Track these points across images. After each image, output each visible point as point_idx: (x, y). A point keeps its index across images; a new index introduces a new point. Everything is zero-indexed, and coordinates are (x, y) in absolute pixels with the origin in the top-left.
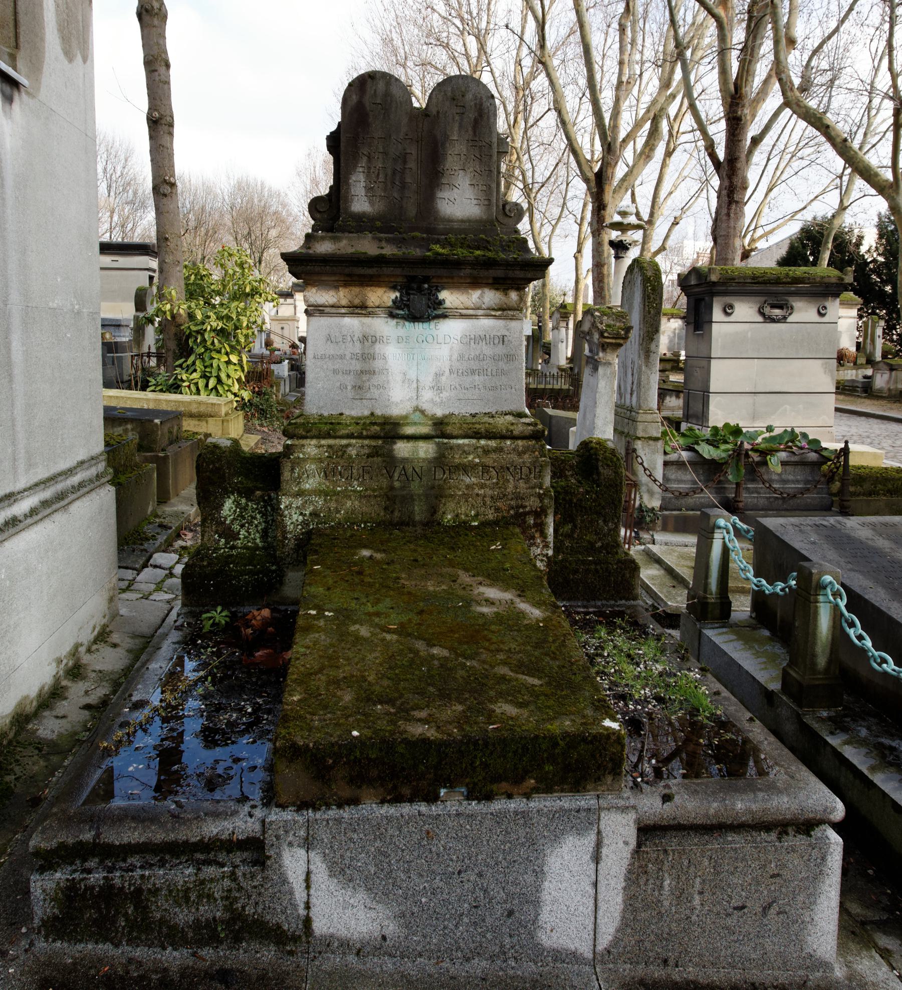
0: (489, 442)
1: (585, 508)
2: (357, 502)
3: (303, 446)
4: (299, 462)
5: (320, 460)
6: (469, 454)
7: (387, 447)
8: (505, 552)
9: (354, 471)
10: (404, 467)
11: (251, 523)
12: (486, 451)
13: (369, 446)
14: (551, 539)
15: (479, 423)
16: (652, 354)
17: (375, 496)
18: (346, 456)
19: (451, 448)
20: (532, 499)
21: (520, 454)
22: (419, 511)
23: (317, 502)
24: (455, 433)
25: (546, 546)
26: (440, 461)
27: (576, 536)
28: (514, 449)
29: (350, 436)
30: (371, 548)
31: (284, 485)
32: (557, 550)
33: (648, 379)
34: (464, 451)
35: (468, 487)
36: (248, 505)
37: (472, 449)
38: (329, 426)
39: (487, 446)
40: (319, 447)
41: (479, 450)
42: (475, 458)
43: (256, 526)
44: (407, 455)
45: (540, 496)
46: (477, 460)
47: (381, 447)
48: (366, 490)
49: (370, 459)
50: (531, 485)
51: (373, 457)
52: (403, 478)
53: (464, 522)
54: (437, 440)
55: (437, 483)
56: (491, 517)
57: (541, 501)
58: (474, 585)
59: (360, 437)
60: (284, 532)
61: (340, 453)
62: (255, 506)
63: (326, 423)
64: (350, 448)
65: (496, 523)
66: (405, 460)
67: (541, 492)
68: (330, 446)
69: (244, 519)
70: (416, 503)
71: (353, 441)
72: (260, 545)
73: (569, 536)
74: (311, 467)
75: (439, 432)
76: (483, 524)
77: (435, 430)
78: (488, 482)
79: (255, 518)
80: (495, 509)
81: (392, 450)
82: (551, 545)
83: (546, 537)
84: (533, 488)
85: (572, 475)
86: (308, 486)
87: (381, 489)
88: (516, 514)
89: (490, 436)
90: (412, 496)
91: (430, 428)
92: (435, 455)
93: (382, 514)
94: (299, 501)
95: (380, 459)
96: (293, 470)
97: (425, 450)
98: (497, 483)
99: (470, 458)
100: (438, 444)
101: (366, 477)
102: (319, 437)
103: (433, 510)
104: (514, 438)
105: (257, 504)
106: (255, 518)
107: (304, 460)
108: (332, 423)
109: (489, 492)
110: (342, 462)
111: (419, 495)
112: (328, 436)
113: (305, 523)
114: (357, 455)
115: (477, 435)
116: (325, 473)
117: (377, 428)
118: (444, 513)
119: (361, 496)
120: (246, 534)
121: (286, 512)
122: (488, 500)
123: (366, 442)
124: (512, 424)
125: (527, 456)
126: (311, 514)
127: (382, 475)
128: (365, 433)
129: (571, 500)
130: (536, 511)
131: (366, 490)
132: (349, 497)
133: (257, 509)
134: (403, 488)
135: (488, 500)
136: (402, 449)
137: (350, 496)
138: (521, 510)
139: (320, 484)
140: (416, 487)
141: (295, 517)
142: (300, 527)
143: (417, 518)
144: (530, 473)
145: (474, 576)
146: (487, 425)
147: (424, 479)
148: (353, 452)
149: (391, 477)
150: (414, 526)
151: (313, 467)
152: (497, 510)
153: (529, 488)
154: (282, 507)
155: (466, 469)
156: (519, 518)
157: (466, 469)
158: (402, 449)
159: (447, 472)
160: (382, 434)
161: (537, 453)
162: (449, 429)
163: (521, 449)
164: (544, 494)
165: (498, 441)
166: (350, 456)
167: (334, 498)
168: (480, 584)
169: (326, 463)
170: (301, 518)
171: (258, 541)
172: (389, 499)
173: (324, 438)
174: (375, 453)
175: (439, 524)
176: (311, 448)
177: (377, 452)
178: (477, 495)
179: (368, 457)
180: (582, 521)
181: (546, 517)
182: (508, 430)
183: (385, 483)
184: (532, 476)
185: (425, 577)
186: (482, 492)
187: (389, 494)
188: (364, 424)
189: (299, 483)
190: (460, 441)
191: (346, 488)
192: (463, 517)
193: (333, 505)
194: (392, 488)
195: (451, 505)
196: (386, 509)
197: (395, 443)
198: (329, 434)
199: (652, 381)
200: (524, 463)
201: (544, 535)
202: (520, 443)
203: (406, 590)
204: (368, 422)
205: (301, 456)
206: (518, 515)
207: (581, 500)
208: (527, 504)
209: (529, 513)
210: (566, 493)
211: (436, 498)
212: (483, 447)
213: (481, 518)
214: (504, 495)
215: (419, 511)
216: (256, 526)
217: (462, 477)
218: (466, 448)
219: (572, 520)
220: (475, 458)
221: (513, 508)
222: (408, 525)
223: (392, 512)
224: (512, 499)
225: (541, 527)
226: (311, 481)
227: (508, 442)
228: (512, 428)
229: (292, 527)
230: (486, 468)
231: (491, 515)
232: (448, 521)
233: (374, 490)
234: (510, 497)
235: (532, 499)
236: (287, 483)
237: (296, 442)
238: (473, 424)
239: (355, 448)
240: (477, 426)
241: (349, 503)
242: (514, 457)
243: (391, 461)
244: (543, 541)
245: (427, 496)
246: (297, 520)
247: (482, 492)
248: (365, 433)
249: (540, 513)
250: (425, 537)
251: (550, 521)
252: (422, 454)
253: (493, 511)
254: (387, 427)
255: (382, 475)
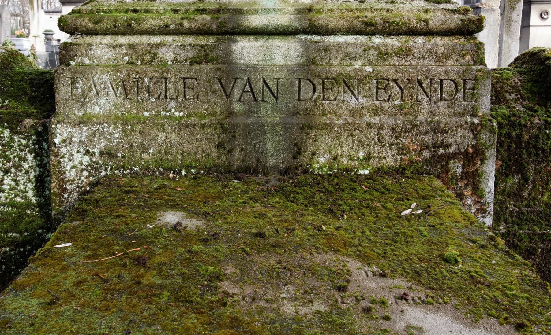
0: (389, 41)
1: (543, 151)
2: (174, 135)
3: (90, 45)
4: (82, 71)
5: (117, 68)
6: (355, 58)
7: (222, 46)
8: (432, 220)
9: (169, 86)
10: (248, 79)
11: (18, 167)
12: (383, 55)
13: (192, 46)
14: (490, 199)
15: (371, 10)
16: (513, 23)
17: (203, 126)
18: (156, 62)
19: (326, 49)
20: (460, 132)
21: (439, 59)
22: (274, 153)
23: (111, 134)
24: (333, 23)
25: (482, 211)
26: (308, 70)
27: (525, 195)
28: (430, 52)
29: (164, 30)
30: (184, 209)
31: (60, 108)
32: (497, 217)
33: (509, 48)
34: (347, 55)
35: (353, 112)
36: (12, 140)
37: (360, 51)
38: (131, 15)
39: (386, 45)
40: (115, 47)
41: (372, 52)
42: (364, 65)
43: (27, 172)
44: (254, 61)
45: (473, 128)
46: (369, 69)
47: (213, 48)
48: (189, 116)
49: (195, 67)
50: (458, 110)
51: (199, 63)
52: (248, 97)
53: (347, 170)
54: (303, 37)
55: (302, 105)
56: (391, 162)
57: (475, 137)
58: (391, 301)
59: (179, 32)
60: (62, 182)
61: (147, 58)
62: (24, 142)
63: (126, 11)
64: (164, 49)
65: (399, 171)
66: (250, 68)
67: (476, 121)
68: (131, 46)
69: (9, 160)
70: (268, 137)
71: (169, 39)
72: (34, 200)
73: (516, 195)
74: (102, 78)
75: (306, 24)
76: (379, 172)
77: (301, 20)
78: (386, 105)
79: (25, 160)
80: (399, 149)
81: (229, 53)
82: (491, 209)
83: (481, 197)
84: (461, 115)
85: (516, 100)
86: (97, 109)
87: (213, 114)
88: (433, 157)
89: (390, 29)
90: (263, 125)
91: (293, 17)
92: (299, 61)
93: (214, 154)
94: (83, 133)
95: (210, 66)
96: (74, 83)
97: (284, 53)
98: (401, 107)
99: (358, 64)
100: (304, 43)
101: (190, 94)
102: (114, 32)
103: (297, 150)
104: (429, 33)
105: (28, 138)
106: (25, 160)
107: (91, 67)
108: (135, 11)
109: (389, 121)
110: (150, 70)
111: (273, 125)
112: (129, 30)
113: (93, 168)
114: (175, 60)
115: (368, 29)
116: (125, 89)
117: (207, 17)
118: (314, 154)
119: (180, 126)
120: (13, 183)
121: (64, 150)
122: (386, 133)
123: (190, 40)
124: (426, 11)
125: (451, 62)
126: (102, 153)
127: (215, 92)
128: (186, 24)
129: (519, 137)
130: (466, 153)
131: (189, 116)
132: (162, 127)
133: (27, 146)
134: (248, 113)
135: (386, 133)
136: (246, 50)
137: (163, 126)
138: (441, 151)
139: (116, 105)
140: (269, 114)
141: (78, 157)
142: (85, 173)
143: (271, 162)
144: (457, 90)
145: (383, 276)
146: (385, 13)
147: (281, 98)
148: (167, 55)
149: (228, 96)
150: (266, 174)
151: (105, 78)
152: (402, 150)
153: (455, 115)
154: (57, 141)
155: (350, 83)
156: (438, 163)
157: (350, 83)
158: (246, 50)
159: (319, 88)
160: (214, 27)
161: (468, 57)
162: (322, 19)
163: (441, 50)
164: (480, 124)
165: (403, 38)
166: (163, 62)
167: (138, 128)
168: (404, 297)
169: (125, 72)
170: (86, 159)
171: (30, 194)
172: (224, 130)
173: (124, 34)
174: (202, 57)
175: (305, 171)
176: (102, 49)
177: (206, 56)
178: (369, 125)
179: (191, 64)
180: (537, 172)
181: (482, 162)
182: (420, 20)
183: (218, 105)
184: (460, 94)
185: (276, 277)
186: (376, 120)
187: (226, 122)
188: (186, 11)
189: (83, 104)
190: (341, 39)
191: (158, 113)
192: (345, 160)
193: (136, 139)
194: (230, 113)
195: (325, 141)
196: (220, 146)
197: (235, 41)
198: (129, 25)
199: (512, 50)
200: (446, 73)
201: (477, 191)
202: (439, 41)
203: (228, 311)
204: (193, 8)
205: (87, 61)
206: (435, 159)
207: (537, 137)
208: (452, 141)
209: (454, 156)
210: (513, 125)
211: (302, 129)
212: (378, 48)
213: (375, 163)
214: (414, 126)
215: (274, 153)
216: (27, 172)
217: (342, 96)
218: (350, 50)
219: (521, 170)
220: (364, 65)
221: (427, 147)
222: (255, 172)
223: (230, 151)
224: (427, 132)
225: (473, 179)
226: (102, 101)
227: (420, 40)
228: (426, 16)
229: (73, 172)
230: (382, 82)
231: (391, 159)
232: (321, 168)
233: (202, 117)
234: (423, 129)
235: (460, 132)
236: (65, 105)
237: (80, 40)
238: (361, 11)
239: (170, 48)
240: (369, 14)
241: (161, 137)
242: (429, 63)
243: (228, 72)
244: (477, 202)
245: (286, 126)
246: (81, 163)
247: (376, 120)
248: (186, 24)
249: (473, 157)
250: (282, 191)
251: (490, 168)
252: (278, 60)
253: (394, 152)
254: (223, 16)
255: (215, 92)
